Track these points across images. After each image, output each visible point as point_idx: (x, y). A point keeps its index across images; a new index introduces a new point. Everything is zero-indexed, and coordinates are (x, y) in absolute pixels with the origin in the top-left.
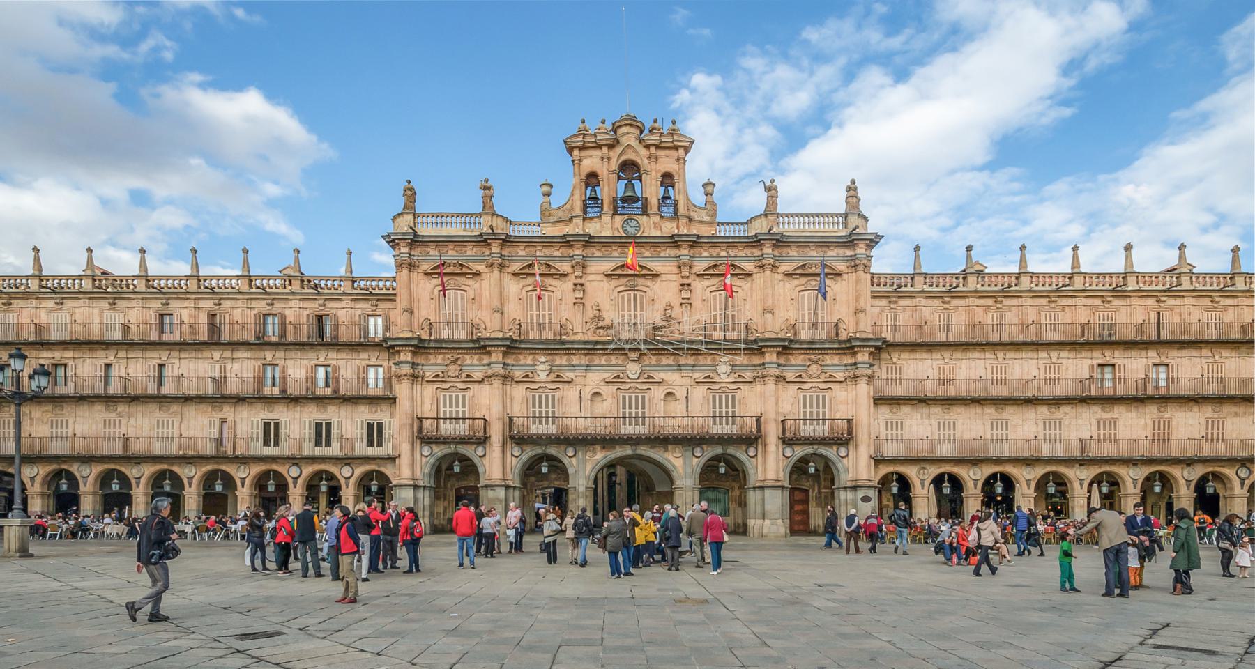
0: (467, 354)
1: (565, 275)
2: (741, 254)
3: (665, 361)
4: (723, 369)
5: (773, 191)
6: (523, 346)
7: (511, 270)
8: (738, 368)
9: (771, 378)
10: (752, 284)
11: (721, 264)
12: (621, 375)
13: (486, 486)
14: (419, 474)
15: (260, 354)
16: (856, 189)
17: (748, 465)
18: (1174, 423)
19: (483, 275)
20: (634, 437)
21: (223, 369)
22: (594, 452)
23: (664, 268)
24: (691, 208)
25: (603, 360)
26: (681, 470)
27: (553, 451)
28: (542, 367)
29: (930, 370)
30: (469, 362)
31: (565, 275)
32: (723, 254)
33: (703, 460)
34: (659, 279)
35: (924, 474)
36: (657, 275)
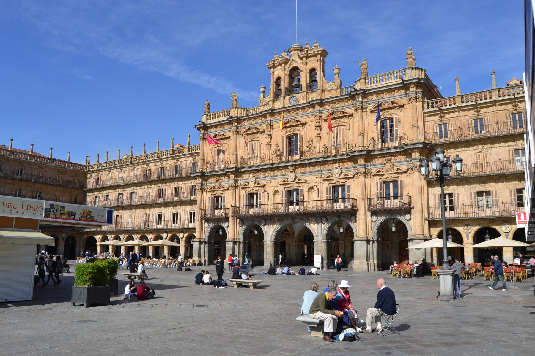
0: (222, 177)
1: (264, 131)
2: (346, 104)
3: (308, 169)
4: (337, 171)
6: (243, 170)
8: (345, 170)
9: (361, 174)
10: (353, 120)
11: (336, 112)
12: (286, 180)
14: (204, 236)
15: (158, 185)
17: (353, 227)
19: (231, 137)
20: (294, 213)
21: (147, 192)
23: (309, 119)
25: (279, 172)
28: (252, 179)
30: (224, 180)
31: (264, 131)
32: (337, 106)
36: (304, 124)
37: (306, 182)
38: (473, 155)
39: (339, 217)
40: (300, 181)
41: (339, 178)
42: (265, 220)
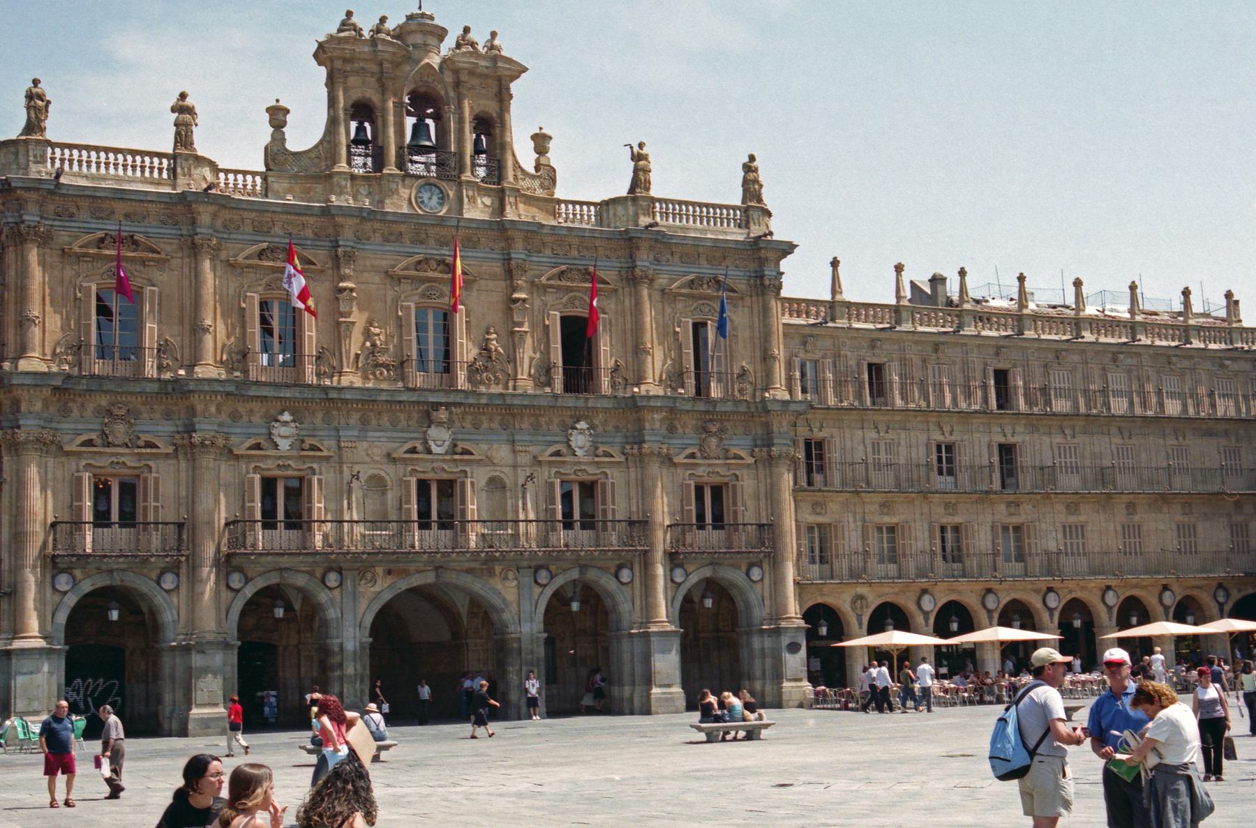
5: (642, 163)
6: (251, 393)
7: (223, 256)
12: (420, 448)
13: (187, 649)
16: (756, 170)
17: (620, 598)
18: (1145, 528)
22: (374, 581)
24: (520, 175)
26: (515, 605)
27: (301, 580)
28: (284, 430)
29: (861, 448)
33: (549, 592)
34: (475, 287)
35: (862, 607)
37: (489, 462)
38: (868, 442)
39: (583, 568)
40: (466, 457)
41: (586, 459)
42: (340, 571)
